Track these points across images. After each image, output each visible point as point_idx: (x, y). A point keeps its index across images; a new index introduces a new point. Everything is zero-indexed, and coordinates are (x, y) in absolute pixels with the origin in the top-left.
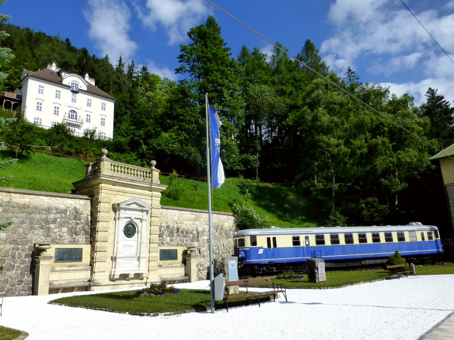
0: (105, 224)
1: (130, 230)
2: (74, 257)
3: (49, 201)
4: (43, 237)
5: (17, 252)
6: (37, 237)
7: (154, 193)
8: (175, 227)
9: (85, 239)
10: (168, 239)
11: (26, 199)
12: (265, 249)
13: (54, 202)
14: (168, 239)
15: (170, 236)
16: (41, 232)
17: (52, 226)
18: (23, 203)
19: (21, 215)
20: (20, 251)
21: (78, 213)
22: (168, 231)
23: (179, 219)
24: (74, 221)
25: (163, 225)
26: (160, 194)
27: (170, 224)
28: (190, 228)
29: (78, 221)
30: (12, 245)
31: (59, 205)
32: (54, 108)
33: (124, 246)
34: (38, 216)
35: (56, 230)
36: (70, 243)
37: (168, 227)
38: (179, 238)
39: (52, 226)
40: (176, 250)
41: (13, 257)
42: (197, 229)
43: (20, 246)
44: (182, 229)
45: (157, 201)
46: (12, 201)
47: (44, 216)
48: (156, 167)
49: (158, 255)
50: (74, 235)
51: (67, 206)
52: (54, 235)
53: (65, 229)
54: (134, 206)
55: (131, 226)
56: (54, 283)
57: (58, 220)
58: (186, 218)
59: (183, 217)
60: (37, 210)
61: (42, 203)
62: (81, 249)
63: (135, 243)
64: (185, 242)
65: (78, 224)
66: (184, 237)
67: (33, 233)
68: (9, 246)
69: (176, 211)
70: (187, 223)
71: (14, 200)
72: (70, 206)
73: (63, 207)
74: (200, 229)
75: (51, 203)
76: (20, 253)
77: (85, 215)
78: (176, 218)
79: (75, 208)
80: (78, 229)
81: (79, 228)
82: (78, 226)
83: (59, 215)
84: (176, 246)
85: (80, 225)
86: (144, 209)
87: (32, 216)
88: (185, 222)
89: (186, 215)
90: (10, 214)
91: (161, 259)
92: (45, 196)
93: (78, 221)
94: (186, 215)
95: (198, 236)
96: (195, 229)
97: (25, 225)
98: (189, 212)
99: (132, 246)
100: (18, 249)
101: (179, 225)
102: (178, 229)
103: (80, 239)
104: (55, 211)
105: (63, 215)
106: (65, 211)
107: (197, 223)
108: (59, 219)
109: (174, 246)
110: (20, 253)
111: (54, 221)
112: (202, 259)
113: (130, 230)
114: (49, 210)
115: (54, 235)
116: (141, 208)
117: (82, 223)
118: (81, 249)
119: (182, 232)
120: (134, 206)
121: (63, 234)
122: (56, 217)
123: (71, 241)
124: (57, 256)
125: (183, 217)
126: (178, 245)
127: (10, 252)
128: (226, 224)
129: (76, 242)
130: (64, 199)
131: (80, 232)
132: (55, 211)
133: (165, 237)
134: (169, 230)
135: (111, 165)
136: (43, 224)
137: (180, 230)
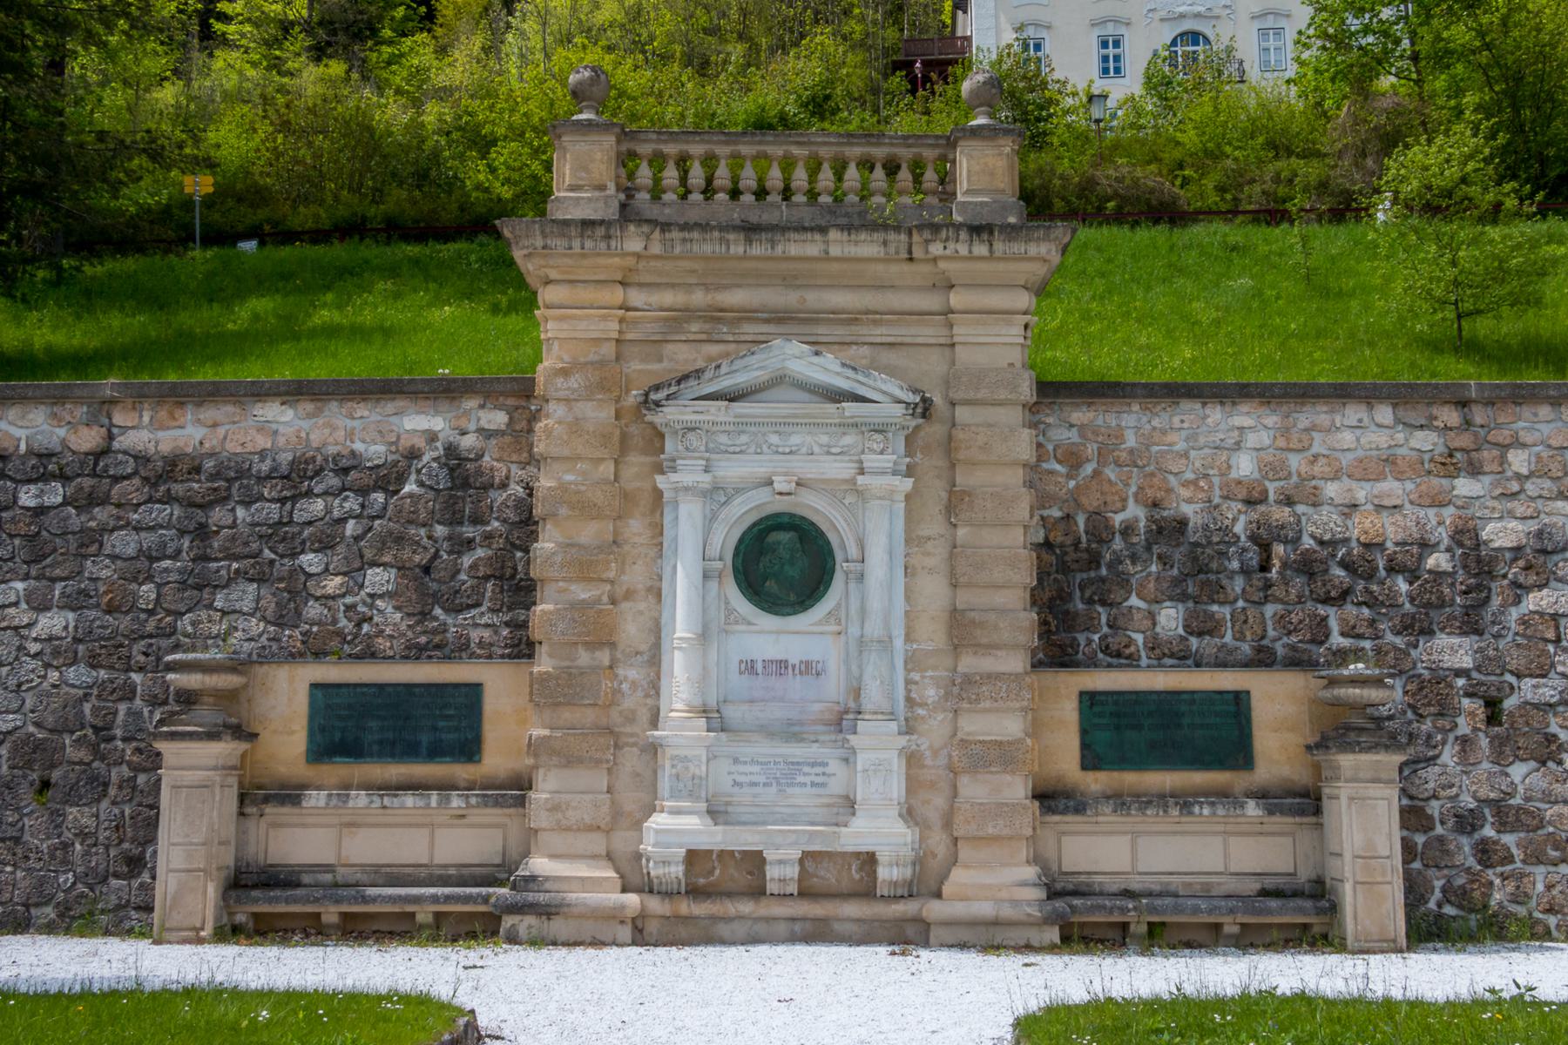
2: (425, 738)
3: (305, 424)
5: (122, 708)
8: (1239, 528)
9: (505, 632)
10: (1170, 619)
13: (334, 429)
14: (1170, 619)
15: (1183, 597)
16: (246, 595)
17: (310, 561)
18: (165, 448)
20: (138, 702)
21: (466, 485)
22: (1164, 560)
23: (1273, 469)
24: (440, 531)
25: (1118, 519)
27: (1188, 510)
28: (1392, 530)
29: (469, 531)
30: (103, 674)
31: (359, 446)
32: (1095, 43)
33: (749, 668)
34: (241, 512)
36: (415, 653)
37: (1169, 530)
38: (1270, 610)
39: (310, 561)
41: (103, 731)
42: (1465, 537)
43: (136, 677)
44: (1308, 542)
46: (116, 445)
47: (273, 511)
50: (438, 611)
51: (405, 443)
53: (378, 578)
55: (784, 537)
56: (306, 879)
57: (351, 528)
58: (1346, 460)
59: (1317, 448)
60: (234, 478)
61: (263, 442)
62: (474, 691)
64: (1337, 640)
65: (469, 544)
66: (1328, 600)
67: (210, 606)
68: (78, 674)
70: (1361, 493)
71: (123, 441)
72: (420, 443)
73: (375, 452)
74: (1501, 533)
75: (316, 439)
76: (135, 715)
77: (517, 490)
78: (1245, 466)
79: (451, 450)
80: (463, 577)
81: (474, 566)
82: (467, 561)
83: (352, 503)
84: (1248, 664)
85: (480, 552)
87: (218, 515)
88: (1331, 490)
89: (1347, 438)
90: (102, 514)
93: (469, 531)
94: (1347, 438)
95: (1478, 595)
96: (1443, 535)
97: (167, 563)
98: (1384, 413)
99: (809, 669)
100: (129, 693)
101: (1281, 514)
102: (1265, 548)
103: (475, 635)
104: (333, 481)
105: (379, 497)
106: (388, 478)
107: (1465, 486)
108: (351, 524)
109: (1221, 664)
110: (135, 715)
112: (1518, 771)
114: (298, 476)
117: (488, 537)
118: (474, 691)
119: (1308, 567)
121: (372, 606)
122: (336, 514)
123: (421, 649)
124: (323, 729)
125: (1317, 448)
126: (1263, 659)
127: (87, 707)
129: (447, 651)
131: (478, 591)
132: (333, 481)
133: (1134, 601)
134: (1178, 555)
136: (267, 554)
137: (1279, 549)
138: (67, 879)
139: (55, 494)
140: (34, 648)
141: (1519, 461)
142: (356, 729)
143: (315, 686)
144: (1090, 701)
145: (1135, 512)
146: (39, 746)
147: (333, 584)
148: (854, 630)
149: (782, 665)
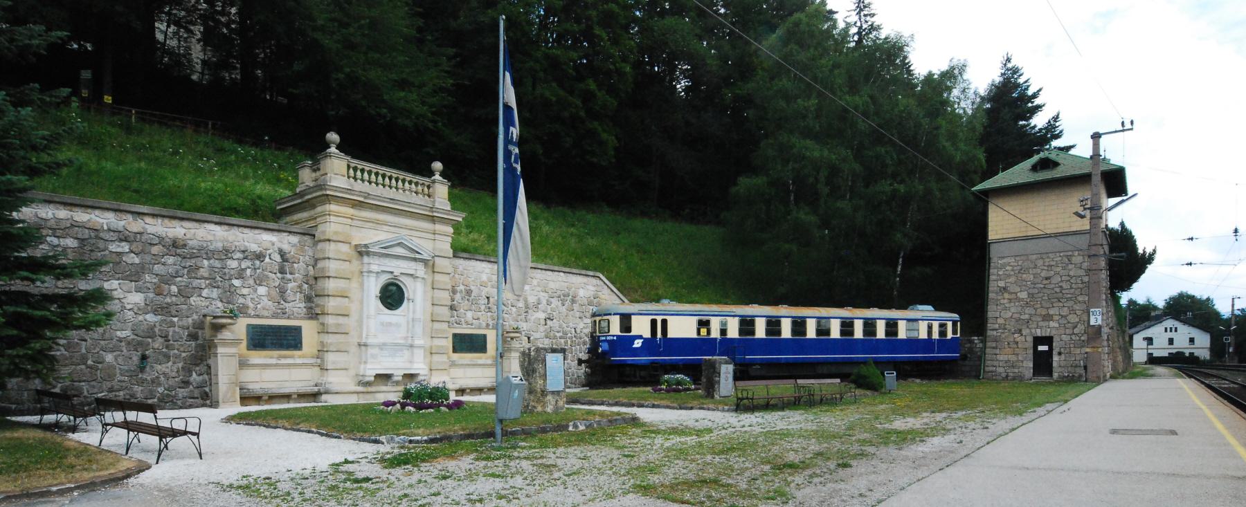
0: (341, 284)
1: (392, 296)
4: (220, 304)
6: (207, 301)
7: (439, 227)
11: (176, 230)
12: (645, 339)
16: (215, 293)
17: (236, 283)
19: (171, 260)
26: (451, 230)
33: (382, 324)
35: (245, 291)
36: (275, 316)
39: (236, 283)
40: (485, 336)
45: (445, 246)
48: (443, 174)
49: (449, 343)
52: (241, 300)
53: (262, 290)
54: (400, 251)
55: (394, 288)
60: (205, 252)
63: (402, 320)
68: (150, 318)
69: (484, 265)
78: (484, 278)
82: (290, 285)
83: (248, 263)
86: (418, 256)
91: (455, 351)
92: (216, 223)
99: (398, 325)
105: (257, 262)
106: (260, 256)
111: (241, 275)
113: (392, 296)
115: (241, 300)
116: (412, 256)
120: (400, 251)
128: (581, 293)
130: (257, 231)
135: (349, 167)
138: (161, 390)
139: (125, 247)
140: (129, 307)
141: (535, 282)
142: (263, 338)
143: (248, 325)
144: (455, 335)
145: (462, 287)
146: (140, 343)
147: (245, 291)
148: (411, 315)
149: (390, 324)
